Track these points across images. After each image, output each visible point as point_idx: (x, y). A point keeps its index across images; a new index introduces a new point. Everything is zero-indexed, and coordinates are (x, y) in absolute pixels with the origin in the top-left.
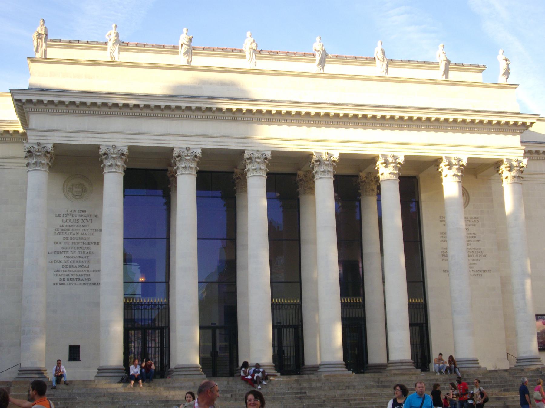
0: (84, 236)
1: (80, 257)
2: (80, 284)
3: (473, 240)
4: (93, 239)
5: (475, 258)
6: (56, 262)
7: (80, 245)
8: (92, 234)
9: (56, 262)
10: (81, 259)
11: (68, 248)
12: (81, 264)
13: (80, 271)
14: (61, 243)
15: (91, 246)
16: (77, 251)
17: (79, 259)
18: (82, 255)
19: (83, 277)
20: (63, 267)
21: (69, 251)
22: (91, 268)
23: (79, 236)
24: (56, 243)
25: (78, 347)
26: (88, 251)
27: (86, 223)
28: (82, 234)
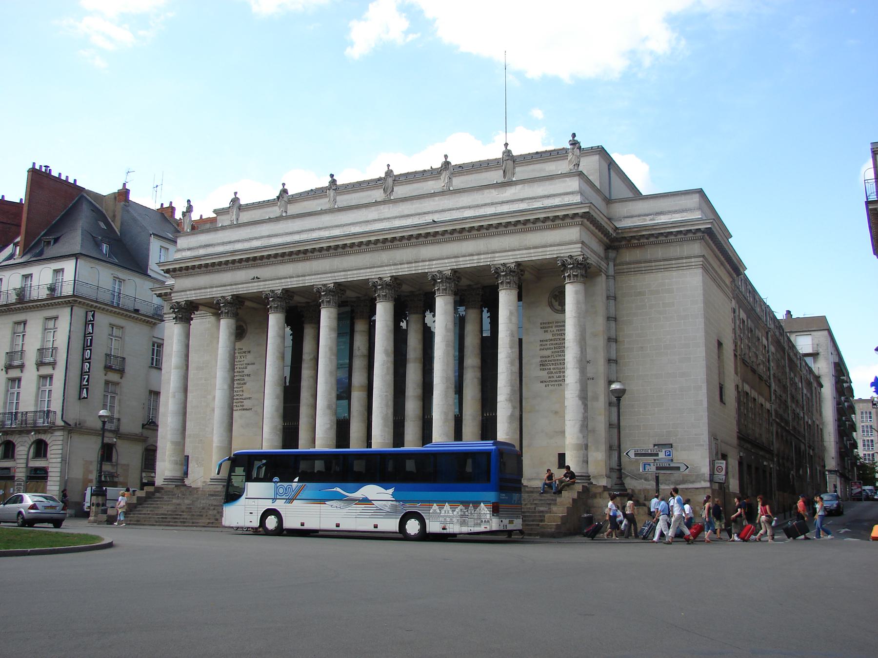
4: (246, 371)
15: (245, 378)
22: (246, 395)
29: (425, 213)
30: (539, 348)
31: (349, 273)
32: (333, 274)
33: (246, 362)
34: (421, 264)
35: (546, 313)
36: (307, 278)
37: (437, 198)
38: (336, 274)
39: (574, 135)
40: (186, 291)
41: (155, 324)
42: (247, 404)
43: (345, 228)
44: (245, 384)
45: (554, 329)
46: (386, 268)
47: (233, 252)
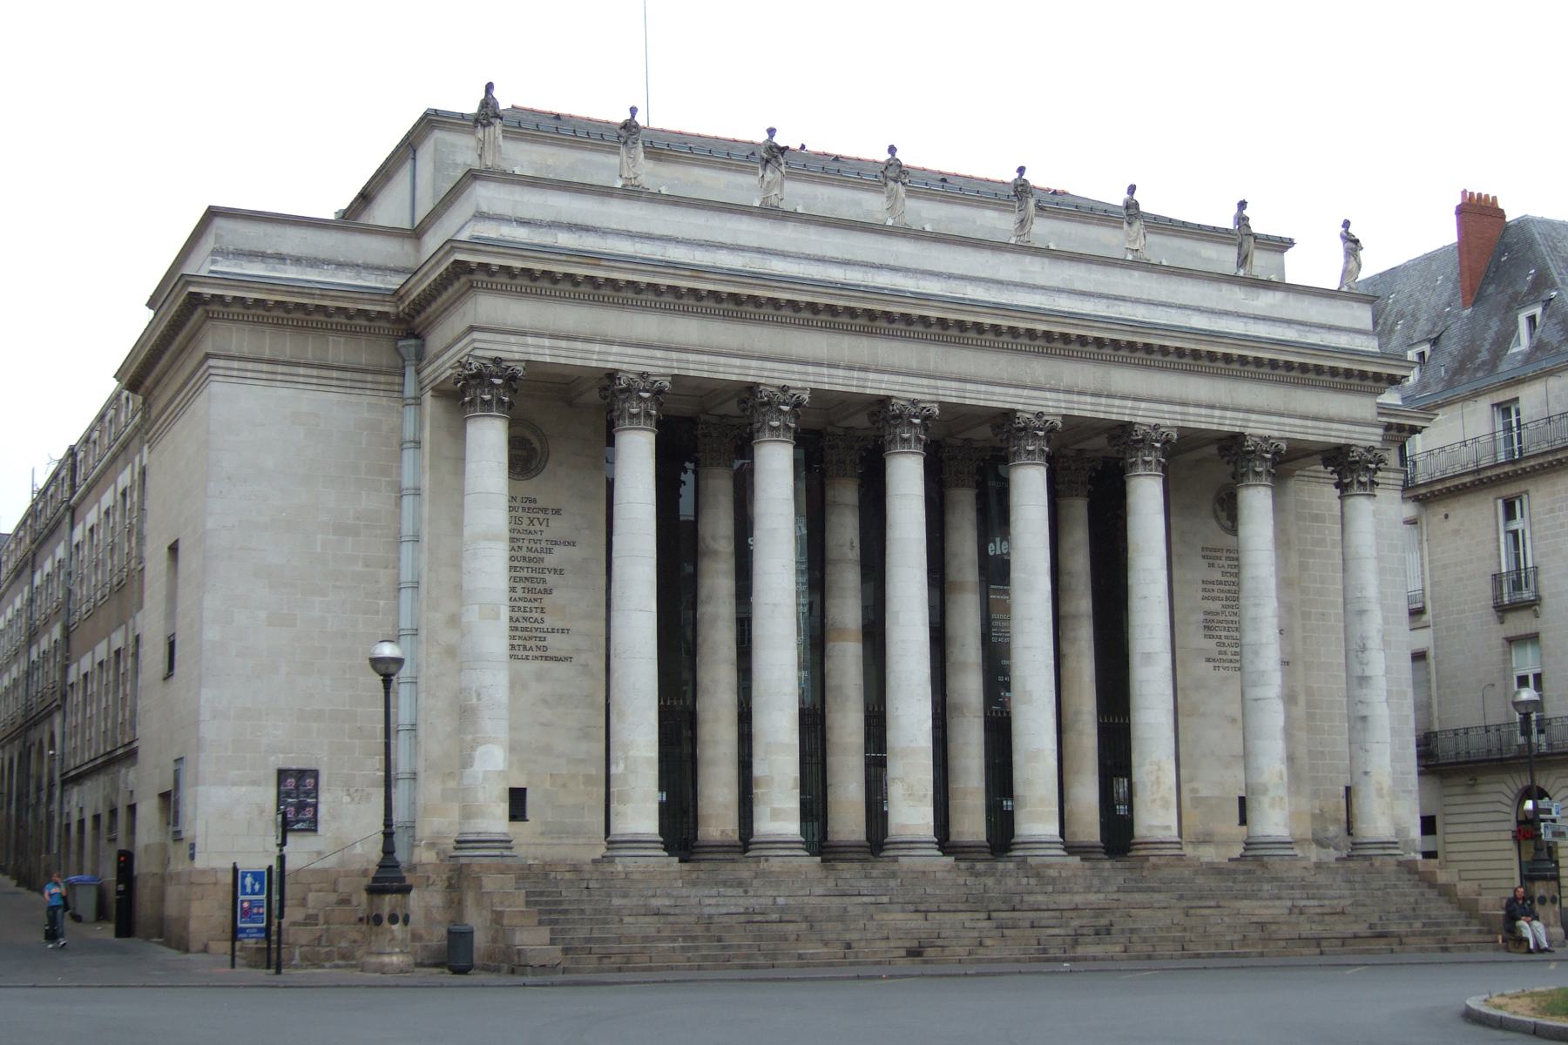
0: (532, 555)
1: (525, 600)
2: (527, 658)
4: (549, 561)
7: (524, 574)
8: (550, 551)
10: (528, 605)
12: (528, 615)
13: (525, 629)
15: (547, 576)
16: (519, 586)
17: (521, 604)
18: (529, 596)
19: (532, 643)
23: (524, 553)
25: (524, 790)
26: (541, 586)
27: (538, 527)
28: (530, 550)
29: (1116, 298)
30: (1201, 594)
31: (969, 386)
32: (932, 382)
33: (545, 536)
34: (1117, 402)
35: (1210, 530)
36: (871, 376)
37: (1136, 274)
38: (940, 383)
39: (1346, 224)
40: (524, 334)
42: (556, 643)
43: (953, 284)
44: (548, 591)
45: (1223, 562)
46: (1048, 395)
47: (697, 271)
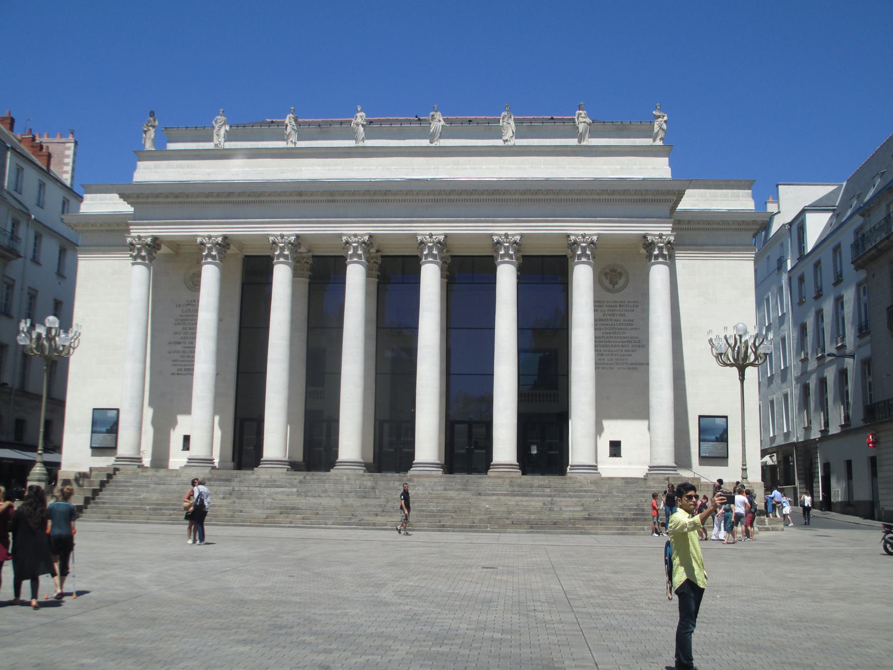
3: (629, 327)
5: (630, 348)
6: (175, 352)
9: (175, 352)
11: (185, 338)
14: (180, 333)
20: (181, 357)
21: (187, 341)
24: (175, 333)
41: (10, 260)
